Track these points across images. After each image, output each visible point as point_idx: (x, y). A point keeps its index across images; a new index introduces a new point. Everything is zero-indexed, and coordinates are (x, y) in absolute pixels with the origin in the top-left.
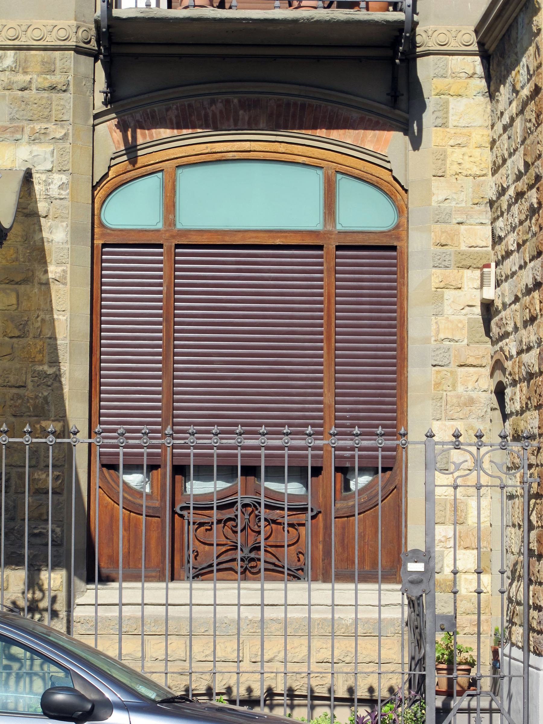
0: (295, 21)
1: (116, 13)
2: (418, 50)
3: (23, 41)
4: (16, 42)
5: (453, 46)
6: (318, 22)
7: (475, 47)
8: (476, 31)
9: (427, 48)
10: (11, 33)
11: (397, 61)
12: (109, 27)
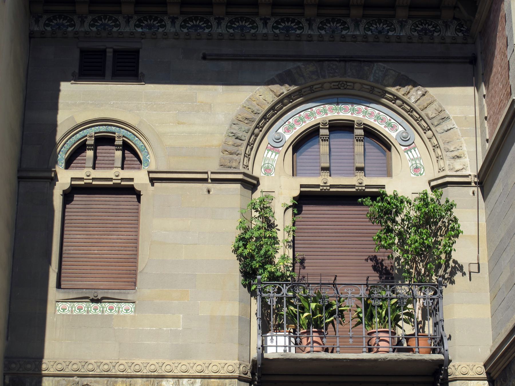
0: (376, 360)
1: (266, 356)
2: (449, 377)
3: (206, 373)
4: (202, 374)
5: (471, 375)
6: (390, 361)
7: (484, 375)
8: (485, 366)
9: (455, 376)
10: (199, 368)
11: (438, 384)
12: (262, 364)
